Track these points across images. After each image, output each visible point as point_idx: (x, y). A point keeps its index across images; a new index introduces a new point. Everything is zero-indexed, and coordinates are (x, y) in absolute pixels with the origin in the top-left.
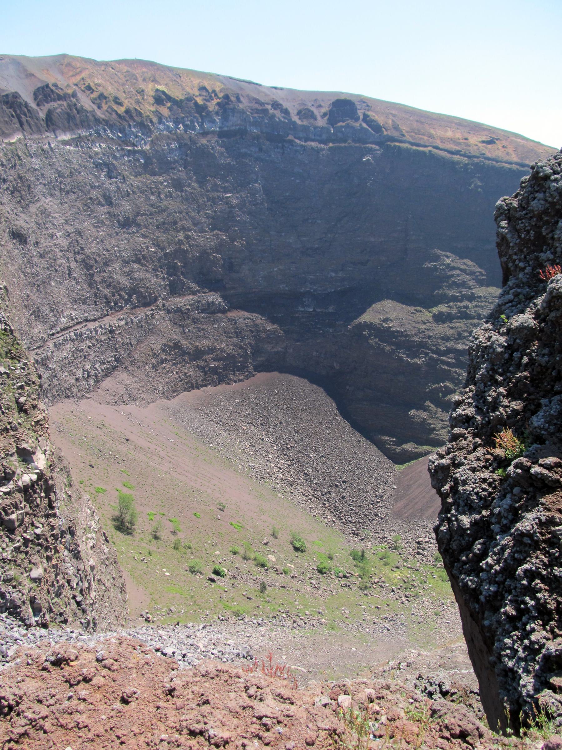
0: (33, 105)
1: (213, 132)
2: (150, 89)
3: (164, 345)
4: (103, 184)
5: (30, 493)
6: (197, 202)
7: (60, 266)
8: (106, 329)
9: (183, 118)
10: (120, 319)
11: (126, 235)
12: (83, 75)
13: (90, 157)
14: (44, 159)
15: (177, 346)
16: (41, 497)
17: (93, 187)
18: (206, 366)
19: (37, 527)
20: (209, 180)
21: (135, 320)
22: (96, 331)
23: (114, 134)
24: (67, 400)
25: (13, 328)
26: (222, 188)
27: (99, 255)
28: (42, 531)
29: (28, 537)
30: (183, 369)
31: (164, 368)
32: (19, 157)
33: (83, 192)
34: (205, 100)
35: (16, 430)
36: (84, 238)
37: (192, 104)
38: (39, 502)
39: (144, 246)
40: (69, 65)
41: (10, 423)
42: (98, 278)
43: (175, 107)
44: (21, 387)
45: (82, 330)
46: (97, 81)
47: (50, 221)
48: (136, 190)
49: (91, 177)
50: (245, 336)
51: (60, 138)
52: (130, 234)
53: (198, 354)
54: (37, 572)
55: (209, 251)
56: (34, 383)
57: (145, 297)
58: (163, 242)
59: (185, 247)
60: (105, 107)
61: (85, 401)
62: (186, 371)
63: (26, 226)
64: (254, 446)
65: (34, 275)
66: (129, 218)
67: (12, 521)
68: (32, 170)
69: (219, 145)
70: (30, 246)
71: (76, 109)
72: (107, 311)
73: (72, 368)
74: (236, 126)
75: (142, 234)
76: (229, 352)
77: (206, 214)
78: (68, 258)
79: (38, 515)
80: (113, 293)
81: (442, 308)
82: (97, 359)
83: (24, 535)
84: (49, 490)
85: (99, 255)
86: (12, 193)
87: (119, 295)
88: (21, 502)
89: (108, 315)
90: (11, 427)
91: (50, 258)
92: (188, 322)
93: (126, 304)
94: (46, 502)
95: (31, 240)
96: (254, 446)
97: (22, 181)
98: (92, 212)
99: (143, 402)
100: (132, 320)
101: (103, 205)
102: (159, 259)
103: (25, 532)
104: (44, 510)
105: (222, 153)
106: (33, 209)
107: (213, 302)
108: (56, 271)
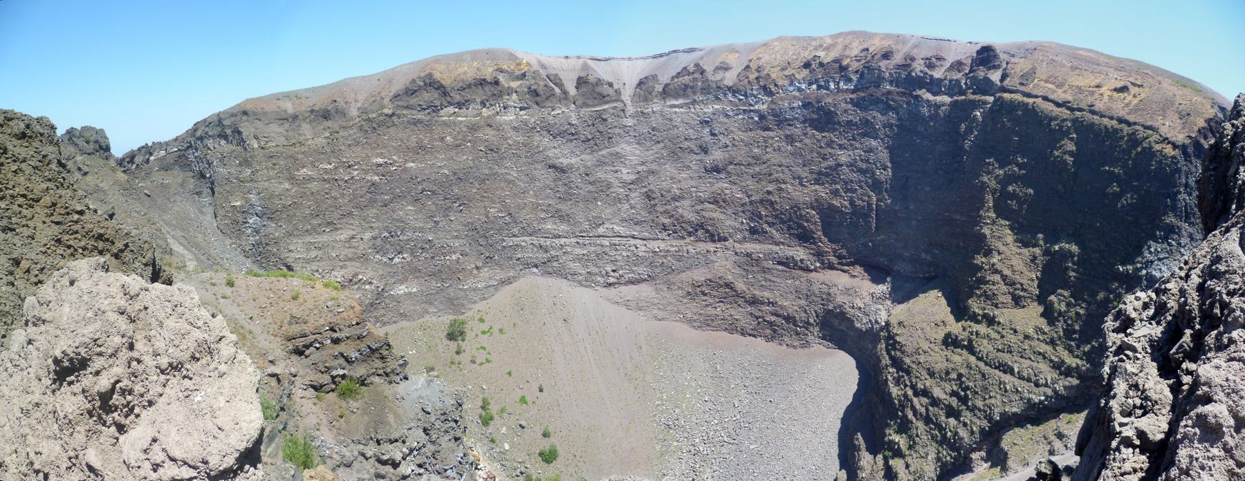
2: (807, 55)
3: (710, 280)
14: (642, 119)
37: (837, 65)
39: (727, 192)
42: (660, 209)
45: (617, 243)
51: (668, 104)
52: (717, 179)
53: (754, 302)
55: (801, 206)
57: (712, 236)
76: (790, 311)
81: (956, 328)
85: (670, 192)
92: (755, 269)
98: (679, 158)
102: (743, 205)
105: (846, 111)
106: (604, 152)
107: (793, 257)
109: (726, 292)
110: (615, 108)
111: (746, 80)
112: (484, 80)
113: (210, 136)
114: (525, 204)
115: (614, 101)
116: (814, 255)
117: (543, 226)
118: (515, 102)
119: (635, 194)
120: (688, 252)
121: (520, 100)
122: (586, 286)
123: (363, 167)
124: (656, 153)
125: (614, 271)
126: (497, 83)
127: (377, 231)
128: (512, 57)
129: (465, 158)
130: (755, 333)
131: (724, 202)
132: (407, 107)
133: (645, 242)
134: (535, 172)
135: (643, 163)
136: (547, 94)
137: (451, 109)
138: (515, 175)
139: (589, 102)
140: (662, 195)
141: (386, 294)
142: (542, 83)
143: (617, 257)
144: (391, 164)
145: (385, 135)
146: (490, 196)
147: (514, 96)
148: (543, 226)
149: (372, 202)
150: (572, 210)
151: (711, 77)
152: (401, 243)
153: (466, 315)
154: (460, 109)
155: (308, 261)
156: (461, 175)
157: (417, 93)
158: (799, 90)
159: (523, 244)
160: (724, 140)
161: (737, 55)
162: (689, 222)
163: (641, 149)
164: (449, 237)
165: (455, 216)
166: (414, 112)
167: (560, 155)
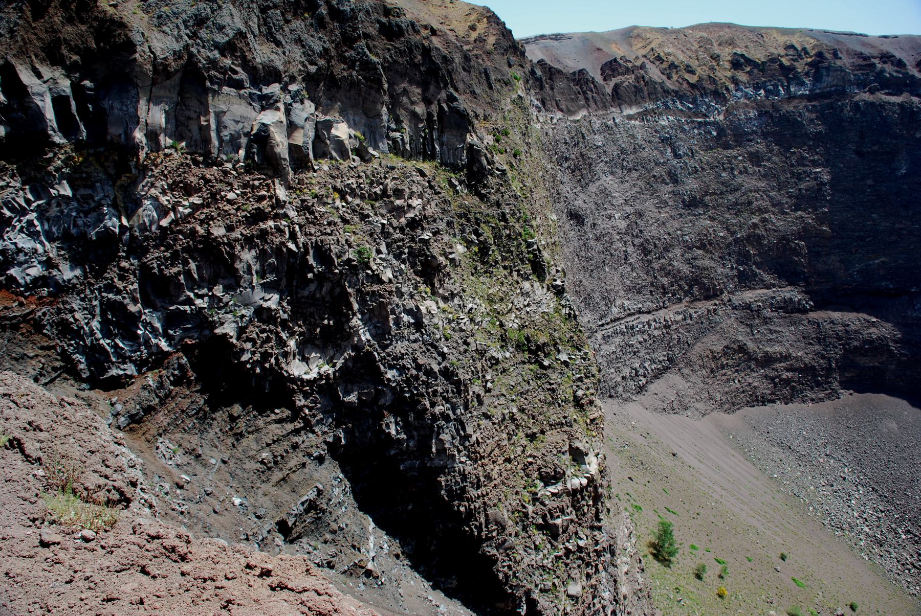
0: (599, 79)
1: (802, 97)
2: (726, 54)
3: (727, 347)
4: (668, 160)
5: (578, 499)
6: (778, 178)
7: (615, 250)
8: (660, 323)
9: (766, 82)
10: (678, 313)
11: (691, 218)
12: (653, 45)
13: (656, 131)
14: (608, 136)
15: (742, 349)
16: (588, 506)
17: (657, 164)
18: (776, 377)
19: (581, 539)
20: (794, 153)
21: (694, 315)
22: (650, 325)
23: (683, 105)
24: (610, 400)
25: (577, 313)
26: (811, 161)
27: (660, 239)
28: (586, 545)
29: (571, 547)
30: (747, 378)
31: (725, 375)
32: (583, 135)
33: (647, 169)
34: (792, 60)
35: (571, 426)
36: (645, 219)
37: (776, 66)
38: (586, 511)
39: (711, 230)
40: (638, 36)
41: (565, 417)
43: (755, 71)
44: (580, 379)
45: (634, 323)
46: (667, 50)
48: (705, 166)
49: (655, 153)
50: (830, 343)
51: (625, 113)
52: (695, 215)
53: (768, 361)
54: (575, 589)
56: (593, 376)
57: (708, 290)
58: (734, 226)
59: (761, 232)
60: (675, 77)
61: (631, 405)
62: (750, 381)
63: (584, 206)
64: (832, 486)
65: (588, 259)
66: (696, 197)
67: (556, 526)
68: (594, 147)
69: (808, 110)
70: (587, 228)
71: (644, 81)
72: (664, 302)
73: (620, 365)
74: (831, 87)
75: (710, 217)
77: (788, 193)
78: (625, 242)
79: (583, 525)
80: (672, 282)
83: (567, 544)
84: (597, 498)
85: (660, 239)
86: (573, 171)
87: (679, 285)
88: (568, 507)
89: (664, 307)
90: (566, 422)
91: (606, 242)
93: (686, 296)
94: (593, 512)
95: (589, 221)
96: (832, 486)
97: (583, 159)
98: (655, 191)
99: (696, 412)
100: (691, 316)
101: (667, 184)
103: (568, 541)
104: (590, 521)
105: (812, 120)
106: (592, 188)
107: (791, 299)
108: (612, 255)
109: (740, 358)
116: (806, 292)
124: (634, 185)
130: (773, 397)
131: (711, 244)
158: (746, 96)
160: (692, 163)
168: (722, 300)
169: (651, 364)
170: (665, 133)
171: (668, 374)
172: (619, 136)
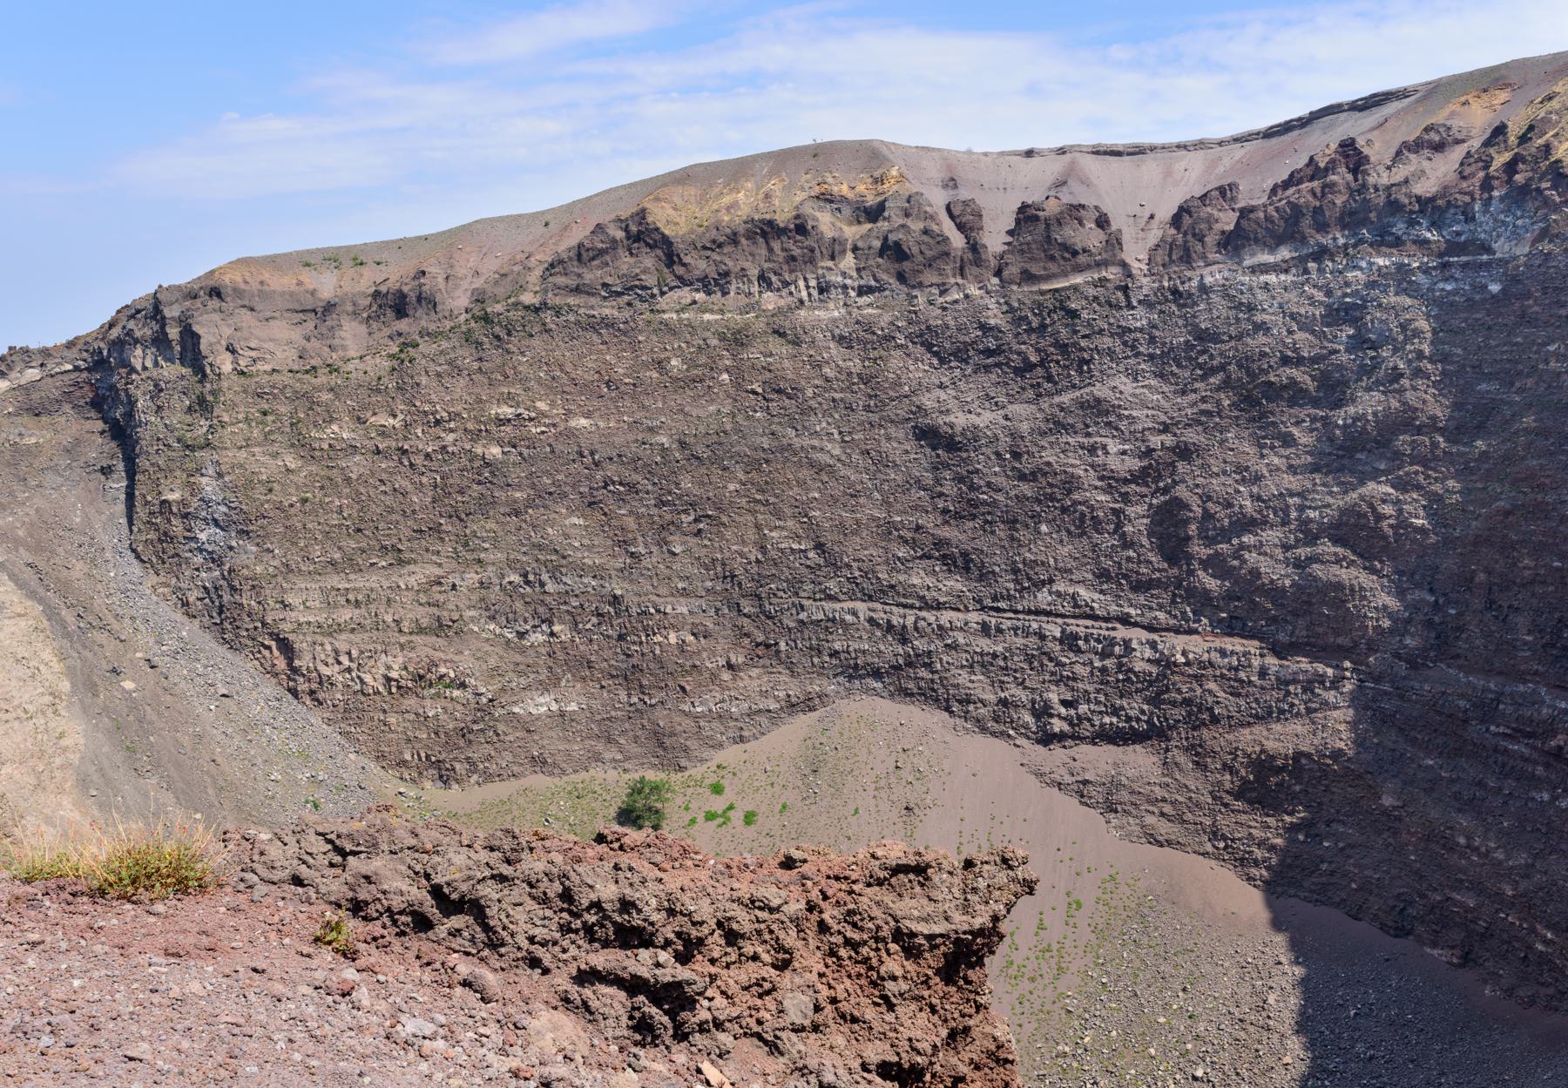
4: (1336, 352)
8: (1162, 653)
13: (1329, 293)
14: (1174, 308)
24: (946, 714)
39: (1388, 510)
42: (1199, 550)
45: (1081, 631)
47: (1108, 424)
51: (1247, 263)
73: (1006, 679)
75: (1399, 477)
78: (1125, 498)
82: (1102, 698)
85: (1229, 505)
91: (1051, 485)
98: (1263, 415)
101: (1316, 403)
106: (1066, 398)
108: (1064, 510)
110: (1103, 282)
111: (1481, 174)
112: (770, 223)
113: (137, 341)
114: (858, 522)
115: (1098, 265)
117: (902, 578)
118: (844, 274)
119: (1141, 509)
120: (1263, 673)
121: (858, 270)
122: (993, 734)
123: (470, 426)
124: (1204, 400)
125: (1064, 703)
126: (801, 228)
127: (490, 568)
128: (870, 156)
129: (710, 412)
132: (577, 290)
133: (1155, 637)
134: (885, 445)
135: (1166, 429)
136: (929, 253)
137: (685, 295)
138: (837, 451)
139: (1036, 269)
140: (1208, 516)
141: (503, 712)
142: (916, 226)
143: (1078, 669)
144: (531, 419)
145: (523, 353)
146: (772, 500)
147: (848, 261)
148: (902, 578)
149: (485, 505)
150: (978, 544)
151: (1380, 177)
152: (548, 599)
153: (687, 774)
154: (709, 293)
155: (334, 630)
156: (700, 450)
157: (608, 258)
159: (849, 618)
161: (1503, 96)
162: (1275, 593)
163: (1165, 389)
164: (663, 591)
165: (683, 543)
166: (593, 301)
167: (952, 404)
168: (1367, 665)
169: (1107, 713)
170: (1346, 295)
171: (1138, 747)
172: (1202, 306)
